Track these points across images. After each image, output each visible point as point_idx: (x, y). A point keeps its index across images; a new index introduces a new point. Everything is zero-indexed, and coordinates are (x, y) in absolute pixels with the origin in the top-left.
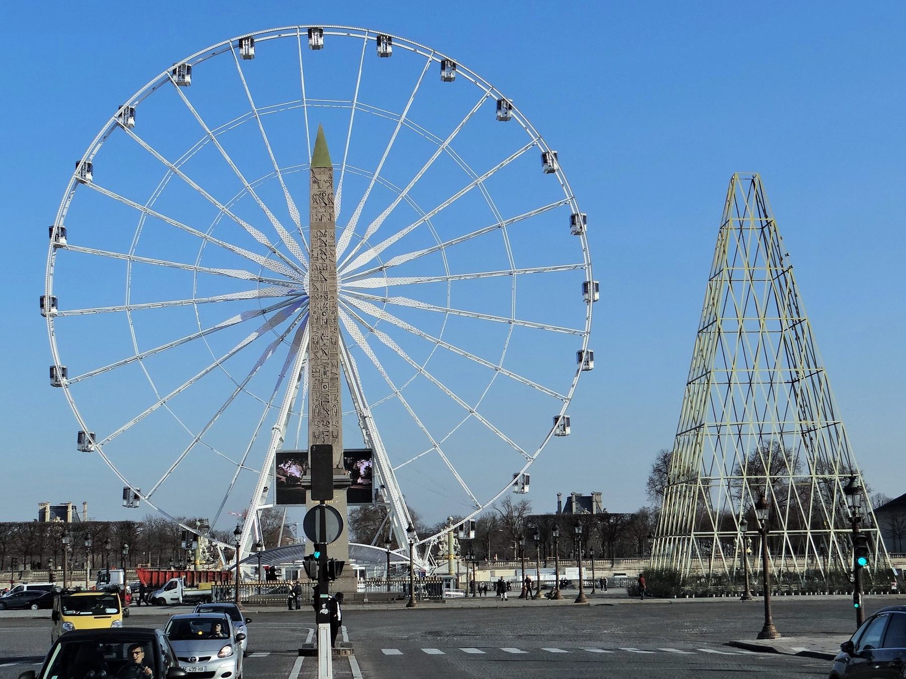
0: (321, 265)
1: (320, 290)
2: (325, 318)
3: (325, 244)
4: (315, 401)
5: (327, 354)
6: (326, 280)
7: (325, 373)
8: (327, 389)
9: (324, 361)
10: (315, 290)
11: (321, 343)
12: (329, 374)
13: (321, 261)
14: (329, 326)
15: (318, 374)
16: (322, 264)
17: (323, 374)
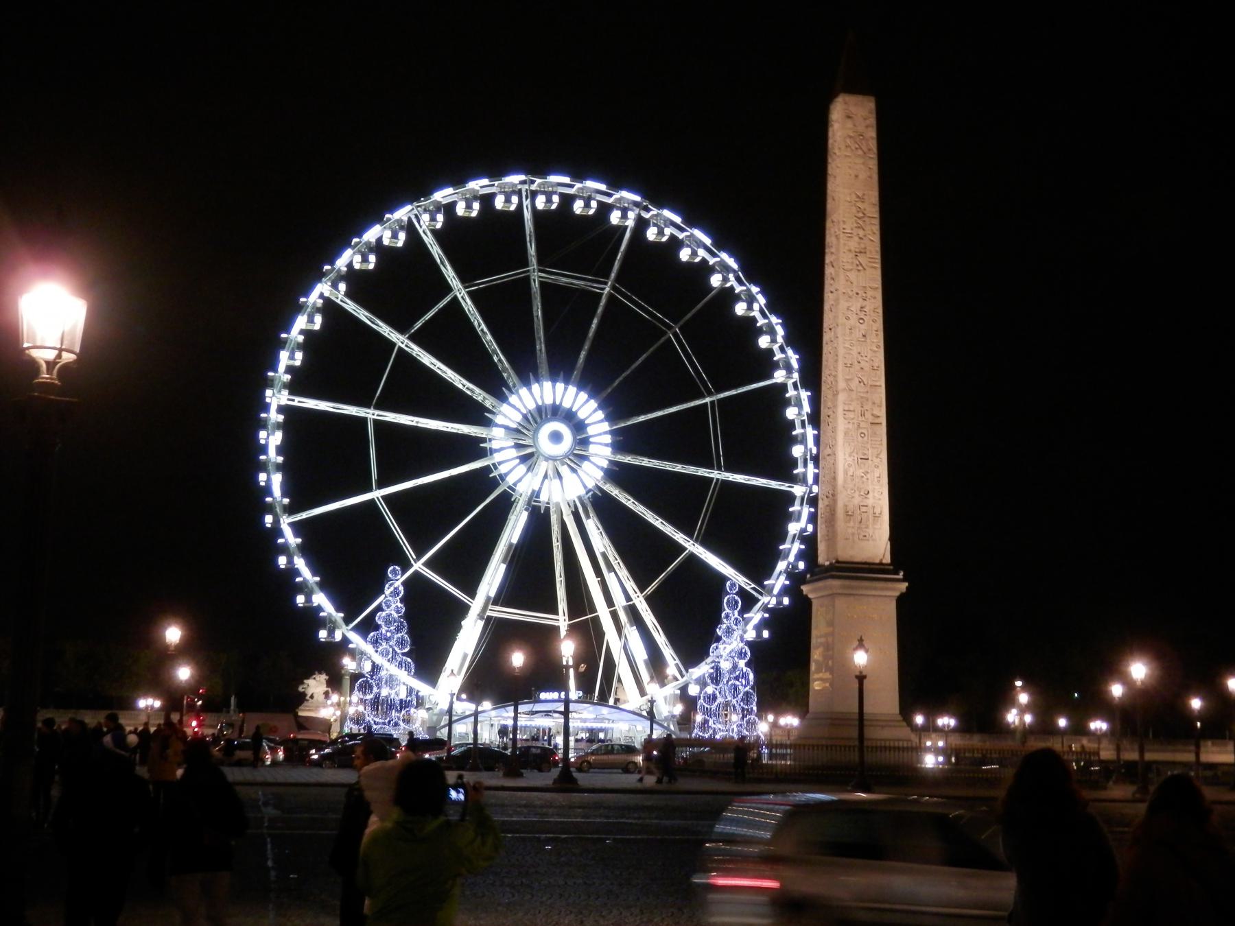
0: (857, 245)
1: (855, 283)
2: (863, 327)
3: (864, 214)
4: (847, 455)
5: (866, 383)
6: (865, 269)
7: (863, 415)
8: (866, 438)
9: (862, 395)
10: (849, 283)
11: (857, 367)
12: (868, 415)
13: (856, 239)
14: (868, 340)
15: (851, 415)
16: (859, 243)
17: (860, 415)
